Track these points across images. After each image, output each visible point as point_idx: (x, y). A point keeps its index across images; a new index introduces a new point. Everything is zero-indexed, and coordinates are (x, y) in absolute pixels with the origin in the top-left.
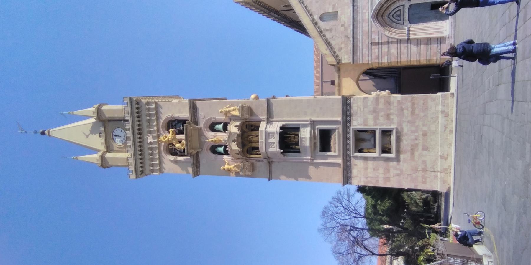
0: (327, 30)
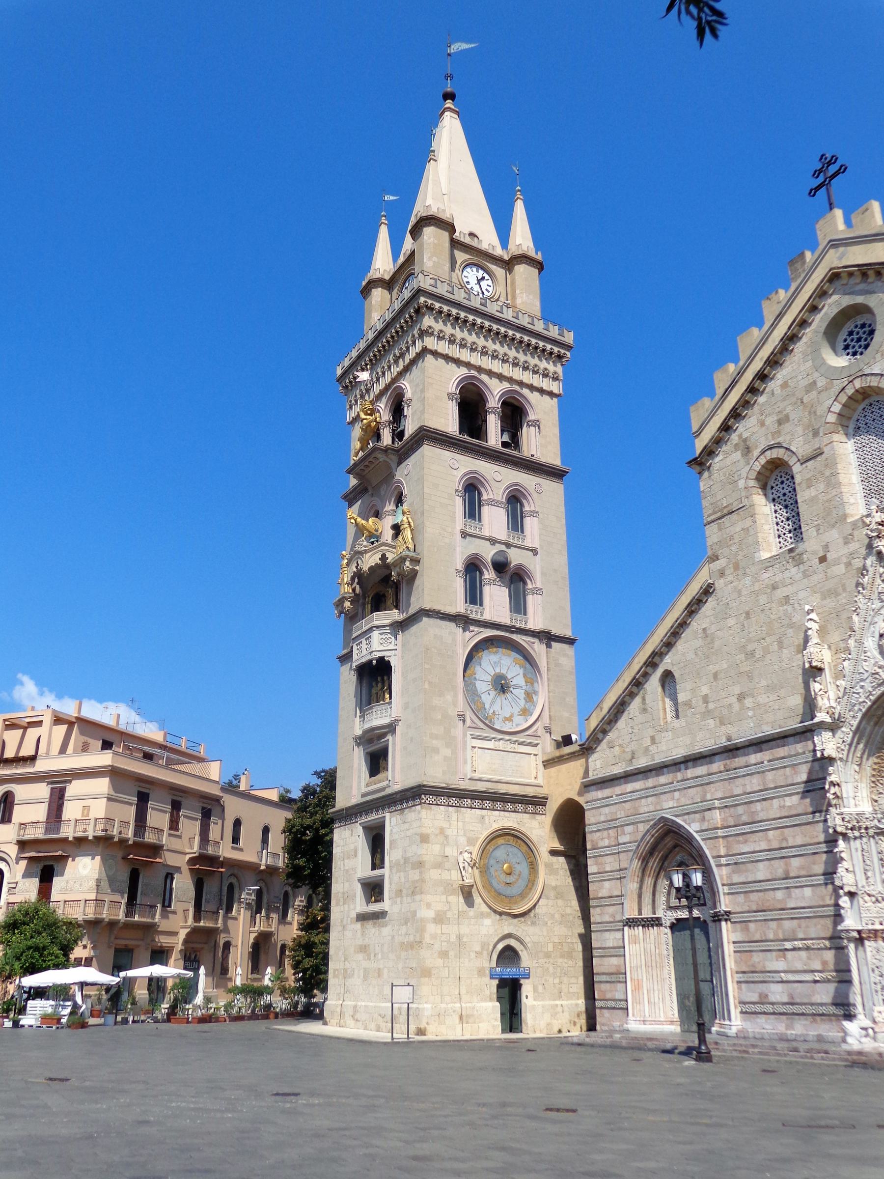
0: (644, 699)
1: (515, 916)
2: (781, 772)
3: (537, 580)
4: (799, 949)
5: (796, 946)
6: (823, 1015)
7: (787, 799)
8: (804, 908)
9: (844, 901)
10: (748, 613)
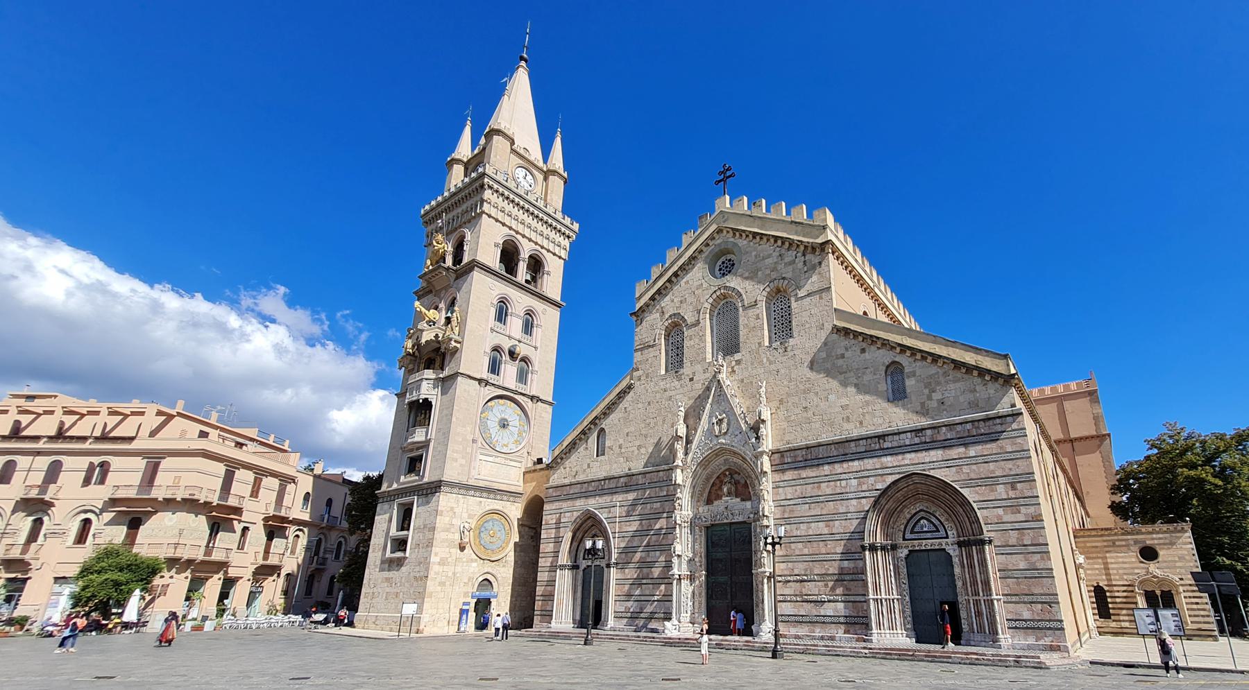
1: (493, 561)
2: (654, 489)
3: (536, 365)
9: (675, 560)
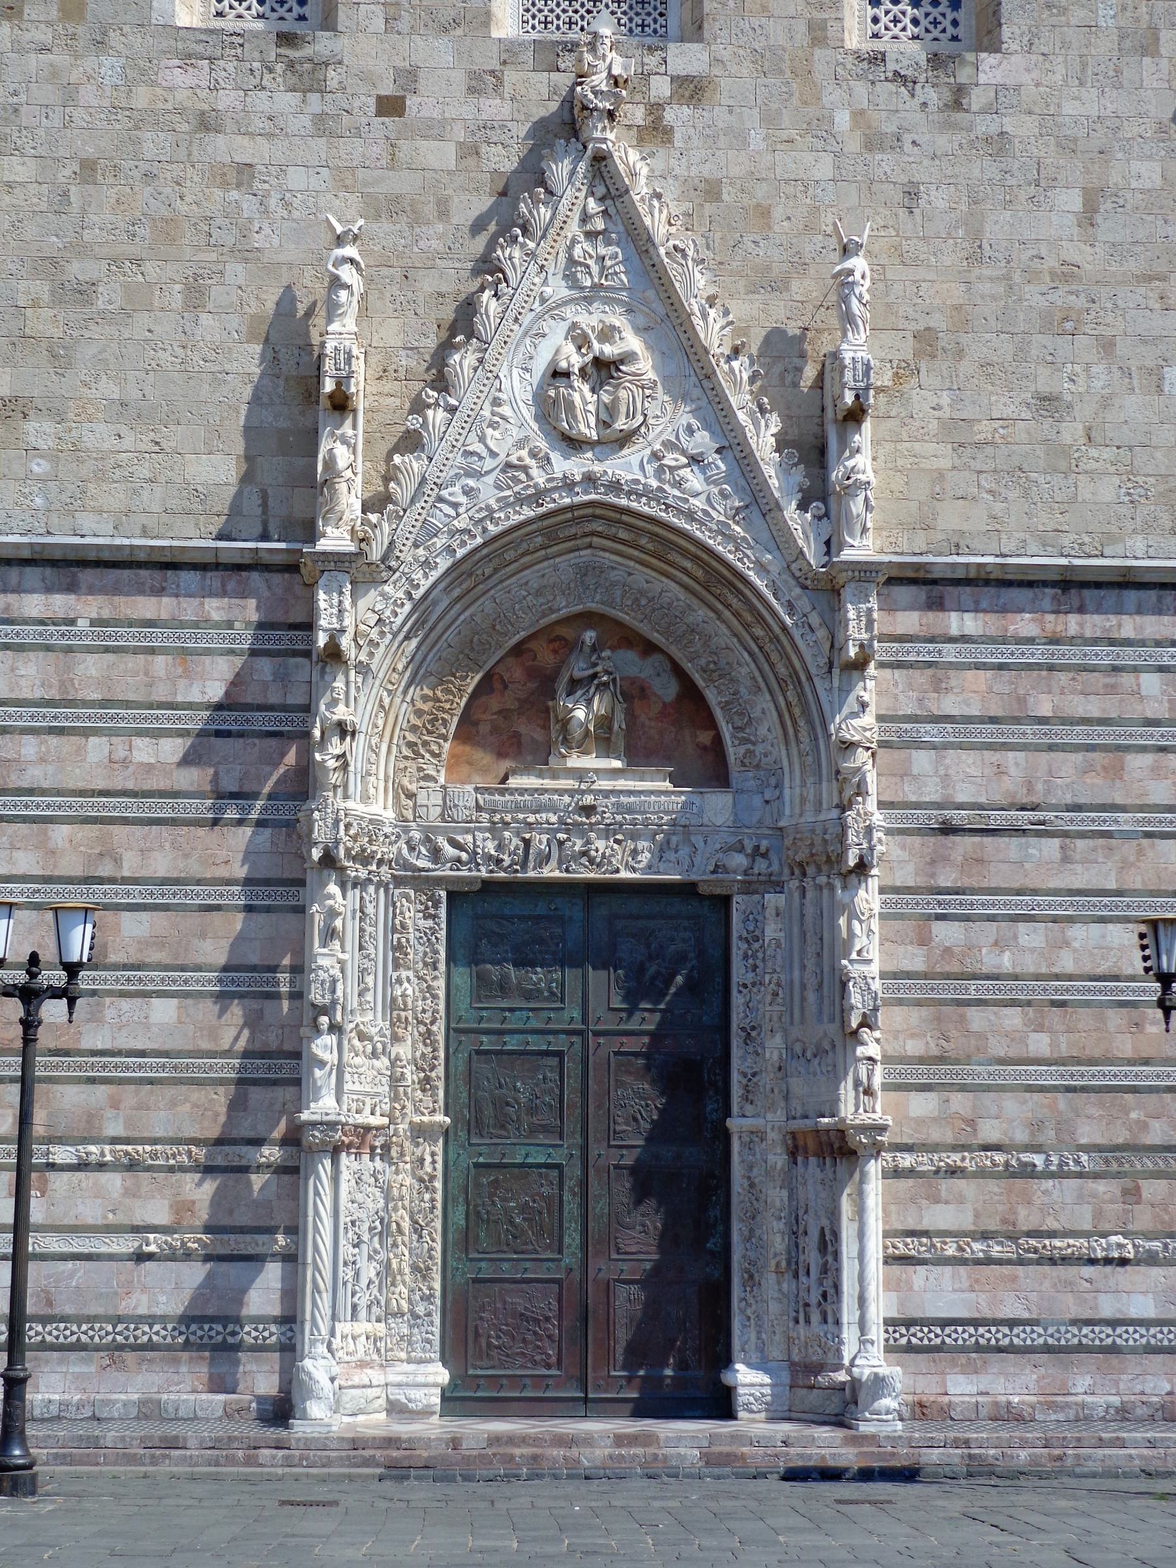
4: (101, 1166)
5: (92, 1158)
6: (150, 1346)
7: (138, 742)
8: (142, 1054)
10: (88, 169)
